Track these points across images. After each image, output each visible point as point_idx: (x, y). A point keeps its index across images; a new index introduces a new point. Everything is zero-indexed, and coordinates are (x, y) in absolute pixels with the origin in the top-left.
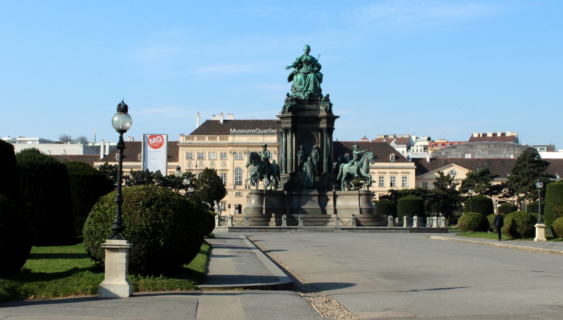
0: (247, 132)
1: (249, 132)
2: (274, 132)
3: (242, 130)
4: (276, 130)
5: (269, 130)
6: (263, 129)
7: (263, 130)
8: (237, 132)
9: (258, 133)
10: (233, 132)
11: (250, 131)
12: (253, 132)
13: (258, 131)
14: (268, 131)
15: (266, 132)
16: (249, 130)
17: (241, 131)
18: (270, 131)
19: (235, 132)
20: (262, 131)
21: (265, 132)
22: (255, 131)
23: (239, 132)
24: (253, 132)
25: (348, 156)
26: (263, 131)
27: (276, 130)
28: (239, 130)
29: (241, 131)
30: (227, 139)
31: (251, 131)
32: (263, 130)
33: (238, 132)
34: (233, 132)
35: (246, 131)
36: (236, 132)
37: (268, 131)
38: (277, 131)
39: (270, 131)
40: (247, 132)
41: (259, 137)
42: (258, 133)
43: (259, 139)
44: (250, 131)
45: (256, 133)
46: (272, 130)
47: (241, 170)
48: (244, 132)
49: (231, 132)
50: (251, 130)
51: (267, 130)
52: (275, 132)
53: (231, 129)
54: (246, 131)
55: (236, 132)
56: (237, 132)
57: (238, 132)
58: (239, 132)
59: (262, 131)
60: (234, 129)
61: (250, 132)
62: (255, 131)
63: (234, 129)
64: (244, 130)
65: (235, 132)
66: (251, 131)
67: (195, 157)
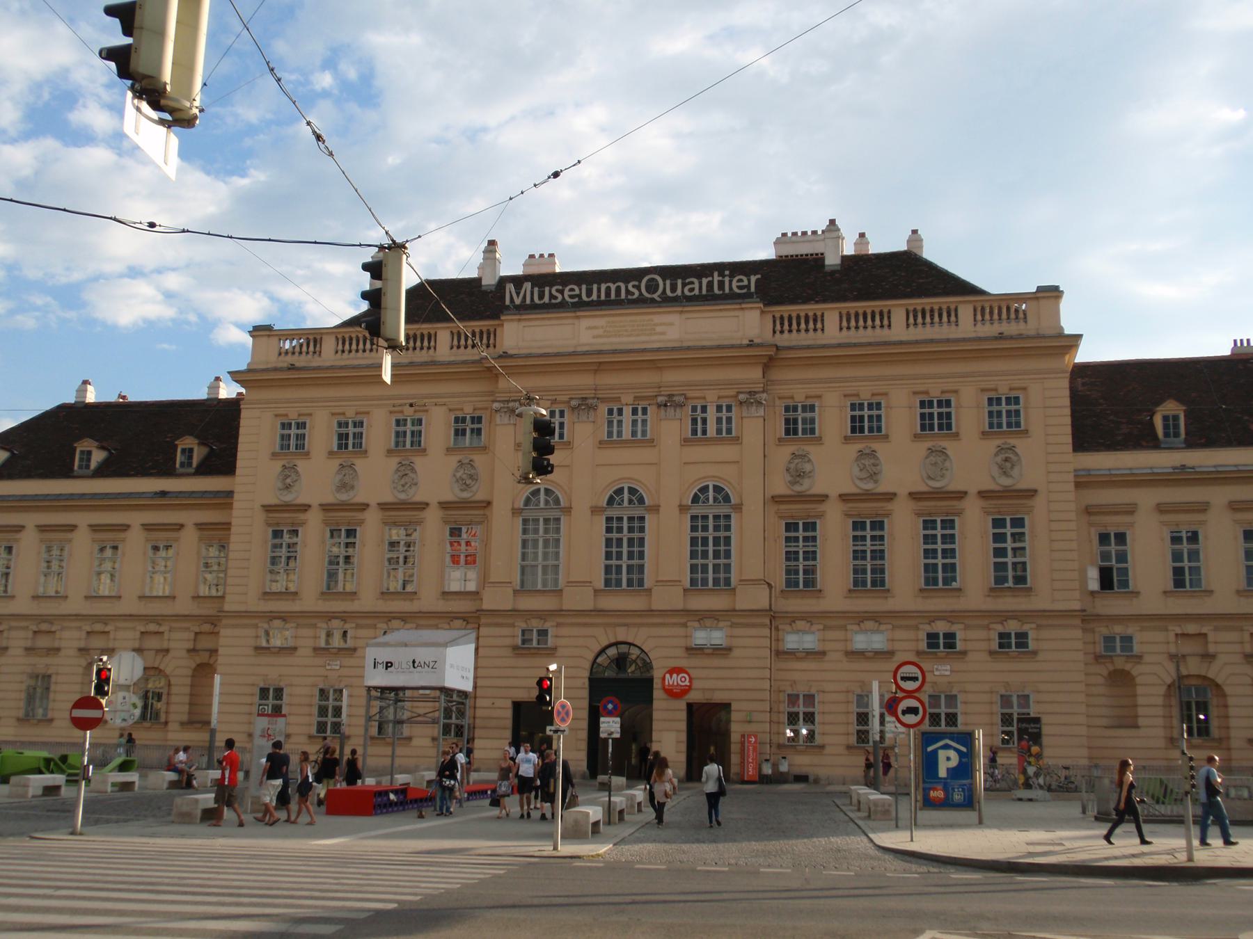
0: (594, 297)
1: (603, 297)
2: (740, 287)
4: (753, 279)
5: (716, 278)
6: (684, 279)
7: (679, 282)
8: (541, 297)
9: (655, 296)
10: (518, 301)
11: (608, 289)
12: (628, 292)
13: (652, 287)
14: (710, 285)
15: (696, 292)
16: (603, 287)
17: (562, 292)
18: (721, 284)
19: (528, 301)
20: (674, 289)
21: (692, 290)
22: (638, 288)
23: (552, 297)
24: (628, 292)
25: (1176, 418)
26: (684, 285)
27: (753, 279)
28: (551, 287)
29: (562, 292)
30: (492, 341)
31: (618, 290)
32: (679, 282)
33: (546, 299)
34: (518, 301)
35: (589, 293)
36: (536, 300)
37: (710, 285)
38: (757, 281)
39: (721, 284)
40: (594, 297)
41: (657, 319)
42: (655, 296)
43: (659, 329)
44: (608, 289)
45: (641, 302)
46: (732, 276)
47: (557, 501)
48: (579, 296)
49: (508, 302)
50: (613, 287)
51: (705, 281)
52: (748, 287)
54: (589, 293)
55: (536, 300)
56: (541, 297)
57: (546, 299)
58: (552, 297)
59: (674, 289)
60: (527, 286)
61: (613, 296)
62: (638, 288)
63: (527, 286)
64: (579, 286)
65: (528, 301)
66: (618, 290)
67: (321, 435)
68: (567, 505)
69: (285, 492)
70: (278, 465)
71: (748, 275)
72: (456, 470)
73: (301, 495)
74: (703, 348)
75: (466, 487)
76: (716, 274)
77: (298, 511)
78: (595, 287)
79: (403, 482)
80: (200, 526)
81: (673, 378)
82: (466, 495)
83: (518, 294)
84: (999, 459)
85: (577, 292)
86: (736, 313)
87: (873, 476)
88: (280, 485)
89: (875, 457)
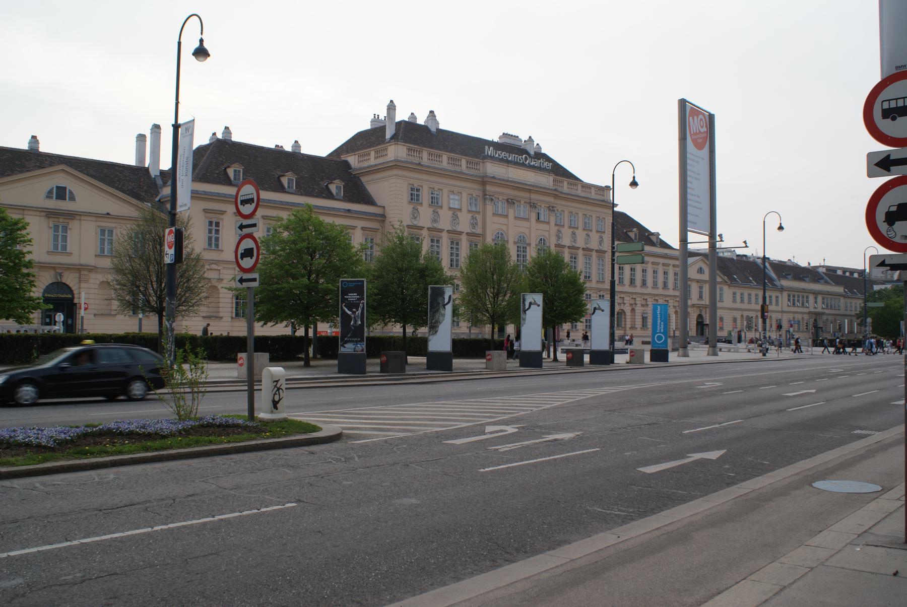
3: (503, 153)
4: (551, 164)
11: (515, 156)
12: (520, 160)
14: (540, 163)
15: (536, 165)
16: (514, 155)
23: (499, 155)
24: (520, 160)
29: (501, 153)
37: (540, 163)
44: (515, 156)
50: (516, 156)
53: (487, 147)
56: (496, 153)
64: (507, 153)
68: (529, 242)
69: (414, 220)
70: (431, 210)
71: (549, 162)
72: (471, 220)
73: (440, 226)
74: (541, 187)
75: (474, 227)
76: (542, 160)
77: (419, 229)
78: (511, 155)
79: (454, 222)
80: (363, 229)
81: (534, 196)
82: (474, 230)
83: (489, 150)
84: (599, 240)
85: (506, 156)
86: (547, 176)
87: (575, 241)
88: (412, 216)
89: (575, 235)
